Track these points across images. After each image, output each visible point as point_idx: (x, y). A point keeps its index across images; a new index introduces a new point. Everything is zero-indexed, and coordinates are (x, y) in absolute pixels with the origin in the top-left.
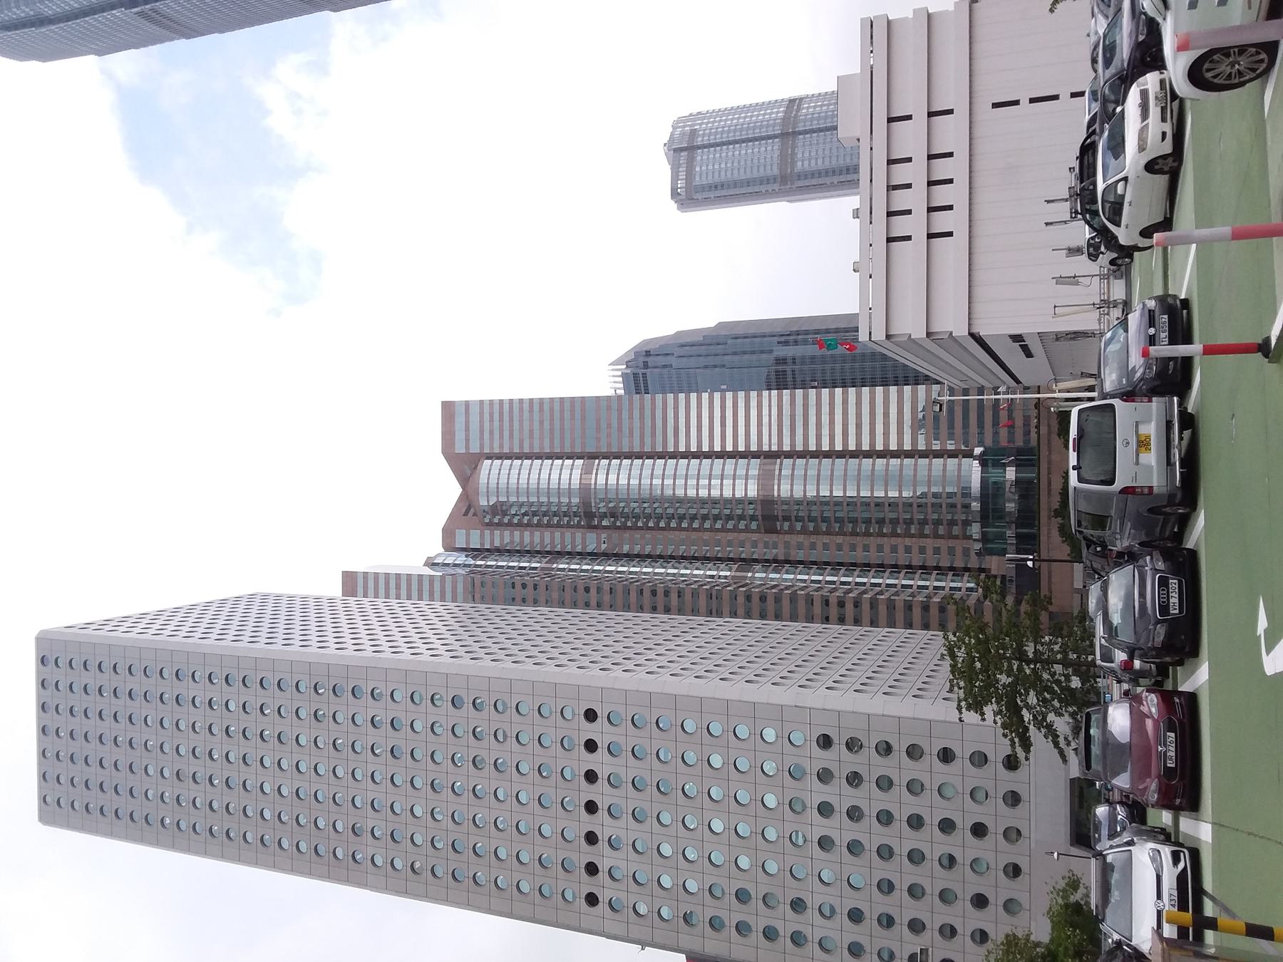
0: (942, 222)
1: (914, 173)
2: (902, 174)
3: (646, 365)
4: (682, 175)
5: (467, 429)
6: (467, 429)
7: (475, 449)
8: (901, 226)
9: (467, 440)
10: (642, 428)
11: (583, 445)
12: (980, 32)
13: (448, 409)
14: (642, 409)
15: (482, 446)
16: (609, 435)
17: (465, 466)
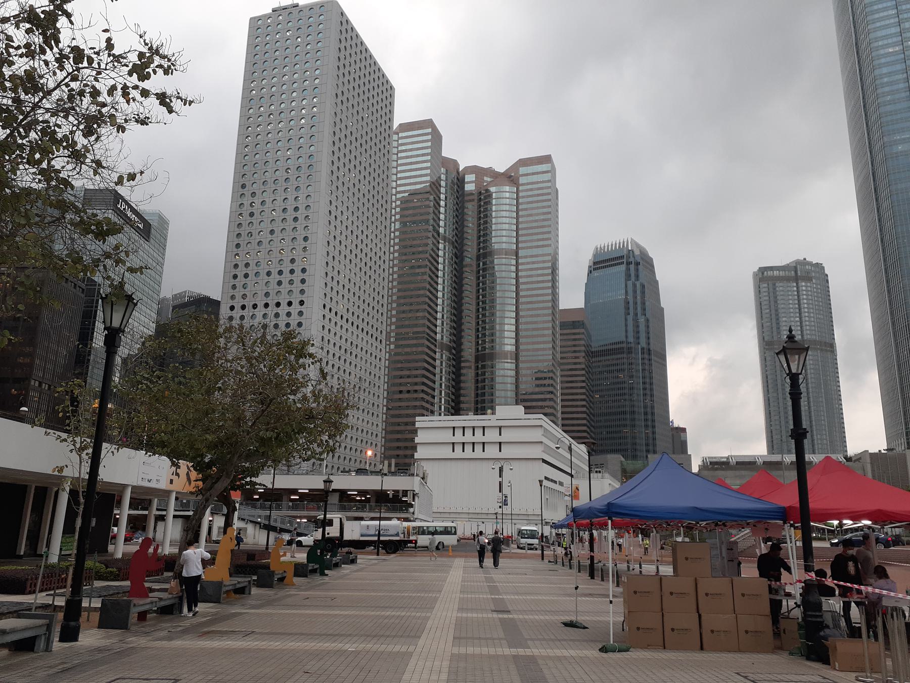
0: (458, 448)
1: (479, 437)
2: (479, 432)
3: (629, 263)
4: (782, 273)
5: (533, 174)
6: (533, 174)
7: (522, 180)
8: (459, 432)
9: (527, 175)
10: (532, 283)
11: (523, 248)
12: (530, 463)
13: (546, 159)
14: (543, 282)
15: (523, 185)
16: (528, 263)
17: (510, 177)
